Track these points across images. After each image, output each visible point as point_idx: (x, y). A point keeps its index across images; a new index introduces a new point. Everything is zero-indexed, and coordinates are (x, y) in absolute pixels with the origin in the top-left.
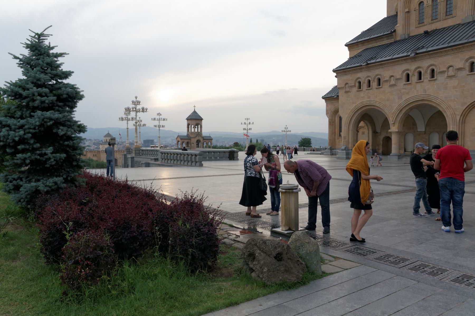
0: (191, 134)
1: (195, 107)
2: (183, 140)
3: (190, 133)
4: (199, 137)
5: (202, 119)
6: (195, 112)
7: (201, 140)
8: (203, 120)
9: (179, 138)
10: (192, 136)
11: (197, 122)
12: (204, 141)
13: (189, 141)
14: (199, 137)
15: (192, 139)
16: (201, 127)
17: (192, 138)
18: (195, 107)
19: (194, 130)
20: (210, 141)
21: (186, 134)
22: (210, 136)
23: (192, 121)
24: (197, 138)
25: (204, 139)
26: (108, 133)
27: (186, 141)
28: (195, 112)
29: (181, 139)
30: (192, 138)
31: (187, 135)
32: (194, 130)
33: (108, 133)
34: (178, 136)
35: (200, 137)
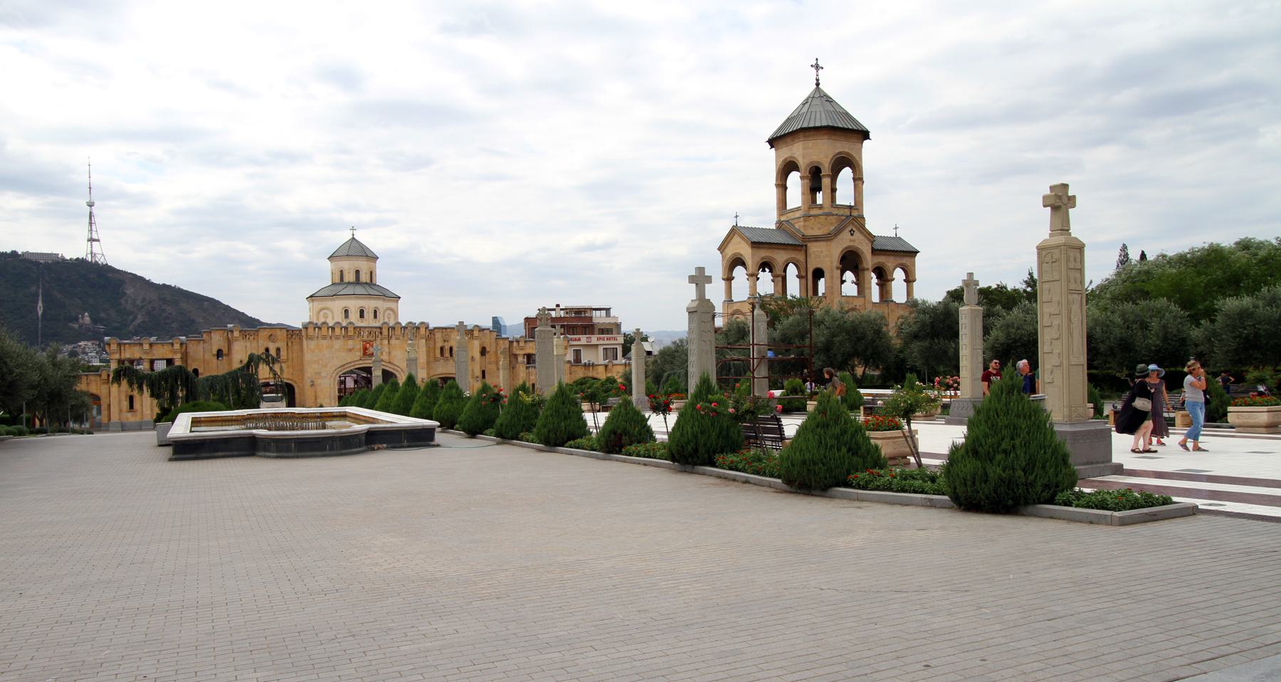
1: (817, 67)
2: (764, 254)
5: (865, 135)
6: (819, 96)
7: (866, 250)
8: (866, 142)
9: (736, 239)
11: (842, 146)
17: (817, 239)
20: (905, 260)
23: (810, 143)
24: (845, 241)
25: (875, 252)
28: (819, 96)
29: (756, 245)
30: (817, 239)
33: (353, 238)
34: (734, 231)
35: (857, 235)
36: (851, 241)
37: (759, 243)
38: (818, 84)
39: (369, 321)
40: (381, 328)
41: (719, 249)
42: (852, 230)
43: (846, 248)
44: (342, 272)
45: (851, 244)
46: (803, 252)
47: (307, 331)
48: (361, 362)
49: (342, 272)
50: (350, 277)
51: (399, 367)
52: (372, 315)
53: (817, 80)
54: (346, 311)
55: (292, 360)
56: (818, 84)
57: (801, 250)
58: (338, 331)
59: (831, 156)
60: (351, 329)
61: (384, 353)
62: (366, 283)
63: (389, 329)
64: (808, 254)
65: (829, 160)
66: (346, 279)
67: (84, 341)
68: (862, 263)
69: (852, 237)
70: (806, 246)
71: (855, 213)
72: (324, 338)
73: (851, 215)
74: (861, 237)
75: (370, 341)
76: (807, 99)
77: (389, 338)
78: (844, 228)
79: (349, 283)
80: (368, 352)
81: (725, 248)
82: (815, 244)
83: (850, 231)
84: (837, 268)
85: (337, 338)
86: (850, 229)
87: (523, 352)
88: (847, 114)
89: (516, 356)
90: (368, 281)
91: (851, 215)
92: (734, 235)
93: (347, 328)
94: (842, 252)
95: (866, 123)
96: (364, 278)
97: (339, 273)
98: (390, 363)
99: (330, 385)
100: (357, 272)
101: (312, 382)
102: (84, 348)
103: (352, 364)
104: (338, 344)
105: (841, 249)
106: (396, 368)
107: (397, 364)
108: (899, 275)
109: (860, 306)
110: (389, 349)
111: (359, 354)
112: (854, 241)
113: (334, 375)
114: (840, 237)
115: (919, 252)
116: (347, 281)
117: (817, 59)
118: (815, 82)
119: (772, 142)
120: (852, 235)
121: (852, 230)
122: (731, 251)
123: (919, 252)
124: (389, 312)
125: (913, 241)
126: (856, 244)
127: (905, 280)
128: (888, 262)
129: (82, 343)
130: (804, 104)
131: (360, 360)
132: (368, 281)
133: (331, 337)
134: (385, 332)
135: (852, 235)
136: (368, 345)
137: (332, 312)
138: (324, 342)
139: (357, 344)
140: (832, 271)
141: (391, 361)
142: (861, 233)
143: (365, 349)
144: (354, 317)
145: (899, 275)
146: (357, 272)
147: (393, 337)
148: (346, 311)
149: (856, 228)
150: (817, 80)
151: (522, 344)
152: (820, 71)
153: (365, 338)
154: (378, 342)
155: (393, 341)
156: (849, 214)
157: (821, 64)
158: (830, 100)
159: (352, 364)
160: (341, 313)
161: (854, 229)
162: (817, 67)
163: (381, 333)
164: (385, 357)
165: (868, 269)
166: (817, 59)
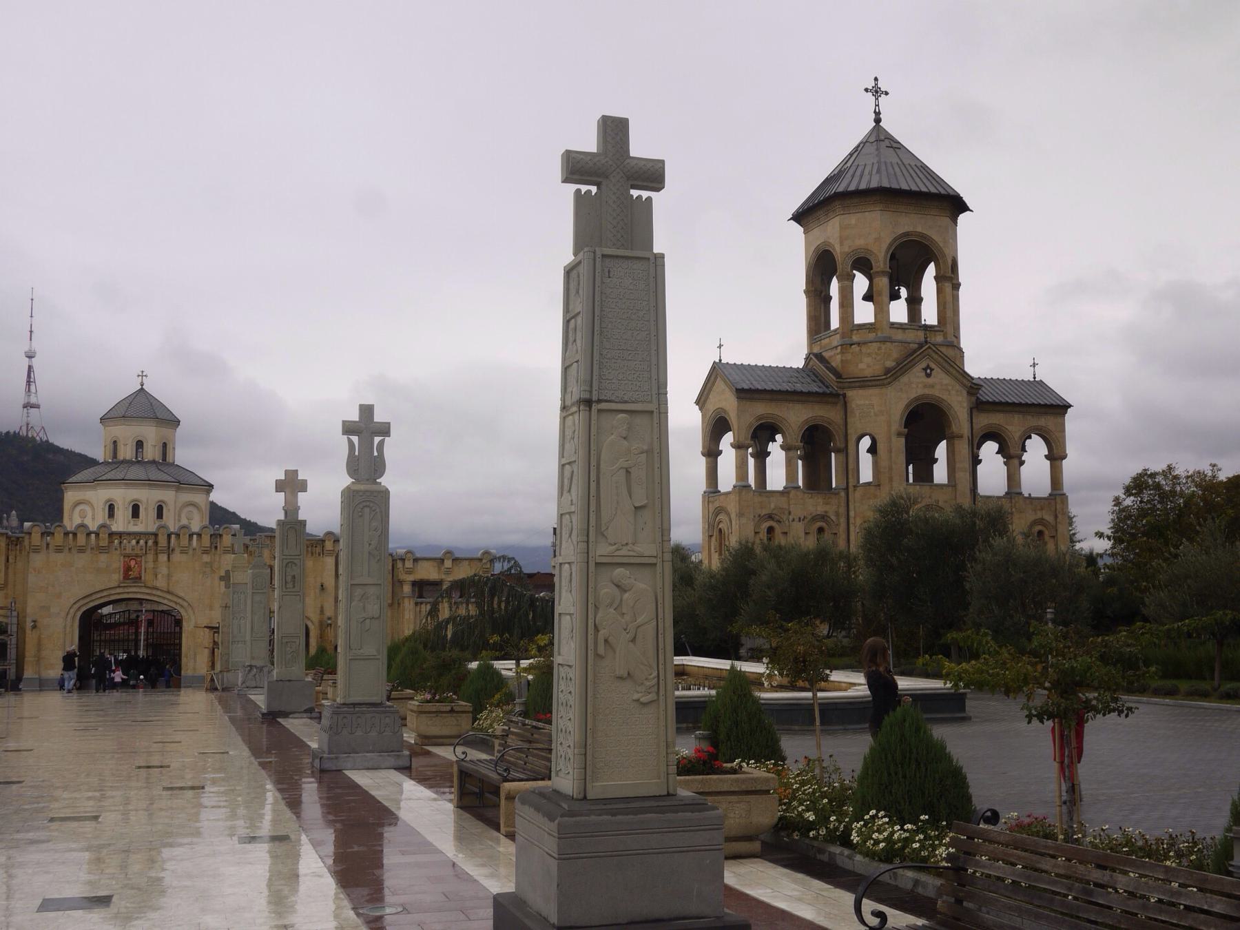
0: (846, 346)
1: (877, 92)
2: (761, 409)
3: (836, 340)
4: (928, 371)
5: (956, 205)
6: (879, 139)
7: (958, 405)
8: (963, 218)
9: (720, 385)
10: (867, 363)
12: (985, 420)
13: (826, 414)
14: (928, 371)
15: (858, 398)
16: (949, 280)
19: (882, 312)
20: (1046, 421)
21: (797, 361)
22: (1038, 385)
23: (852, 219)
24: (914, 386)
26: (142, 389)
27: (797, 417)
28: (879, 139)
29: (745, 394)
30: (864, 383)
31: (808, 370)
32: (882, 312)
33: (142, 389)
36: (925, 387)
37: (750, 391)
38: (878, 121)
39: (147, 523)
40: (156, 535)
41: (697, 402)
42: (928, 367)
43: (916, 399)
44: (115, 442)
45: (927, 391)
47: (30, 538)
48: (120, 590)
49: (115, 442)
50: (126, 452)
51: (184, 600)
52: (153, 513)
53: (877, 114)
54: (111, 508)
55: (14, 586)
56: (878, 121)
57: (836, 403)
58: (81, 539)
59: (888, 240)
60: (104, 534)
61: (159, 576)
62: (154, 462)
63: (169, 536)
64: (849, 410)
65: (885, 246)
66: (121, 456)
68: (950, 426)
69: (930, 381)
70: (844, 396)
71: (939, 339)
72: (59, 550)
73: (926, 342)
74: (947, 380)
75: (137, 556)
76: (858, 146)
77: (169, 551)
78: (912, 365)
79: (124, 462)
80: (132, 574)
81: (705, 401)
82: (861, 392)
83: (925, 369)
84: (899, 434)
85: (81, 550)
86: (924, 365)
87: (411, 578)
88: (924, 168)
89: (401, 583)
90: (159, 458)
91: (926, 342)
92: (716, 378)
93: (98, 534)
94: (907, 406)
95: (956, 178)
96: (151, 453)
97: (112, 446)
98: (168, 592)
99: (65, 627)
100: (140, 444)
101: (34, 621)
103: (105, 593)
104: (81, 560)
105: (905, 402)
106: (179, 601)
107: (182, 594)
108: (1036, 449)
109: (946, 502)
110: (169, 568)
111: (116, 578)
112: (932, 386)
113: (72, 611)
114: (904, 379)
115: (1070, 406)
116: (122, 458)
117: (876, 79)
118: (873, 116)
119: (802, 216)
120: (928, 376)
121: (928, 367)
122: (712, 405)
123: (1070, 406)
124: (191, 508)
125: (1060, 384)
126: (936, 392)
127: (1046, 457)
128: (1013, 425)
130: (851, 155)
131: (119, 587)
132: (159, 458)
133: (70, 549)
134: (162, 541)
135: (928, 376)
136: (133, 563)
137: (93, 509)
138: (59, 558)
139: (115, 561)
140: (889, 440)
141: (171, 589)
142: (947, 372)
143: (128, 569)
144: (122, 514)
145: (1036, 449)
146: (140, 444)
147: (178, 550)
148: (111, 508)
149: (938, 364)
150: (877, 114)
151: (409, 564)
152: (883, 99)
153: (128, 551)
154: (150, 557)
155: (177, 557)
156: (923, 339)
158: (895, 145)
159: (105, 593)
160: (104, 509)
161: (933, 365)
162: (877, 92)
163: (156, 543)
164: (161, 583)
165: (961, 437)
166: (876, 79)
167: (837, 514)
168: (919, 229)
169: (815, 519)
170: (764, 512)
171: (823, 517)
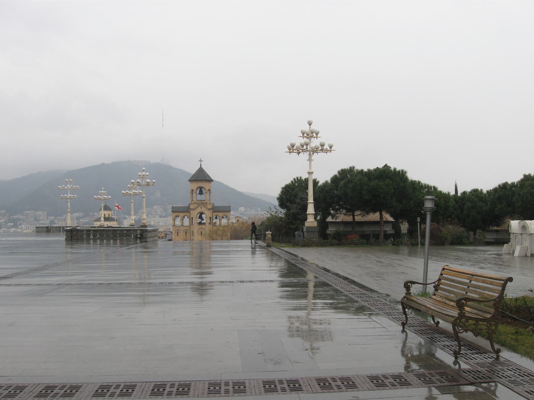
1: (201, 161)
2: (176, 214)
18: (201, 161)
38: (201, 166)
45: (201, 211)
46: (189, 213)
53: (201, 165)
56: (201, 166)
59: (196, 187)
65: (195, 188)
67: (156, 206)
100: (105, 215)
102: (156, 209)
112: (202, 210)
129: (155, 207)
132: (108, 217)
150: (201, 165)
157: (200, 160)
167: (189, 229)
168: (202, 185)
169: (185, 230)
170: (176, 229)
171: (186, 230)
